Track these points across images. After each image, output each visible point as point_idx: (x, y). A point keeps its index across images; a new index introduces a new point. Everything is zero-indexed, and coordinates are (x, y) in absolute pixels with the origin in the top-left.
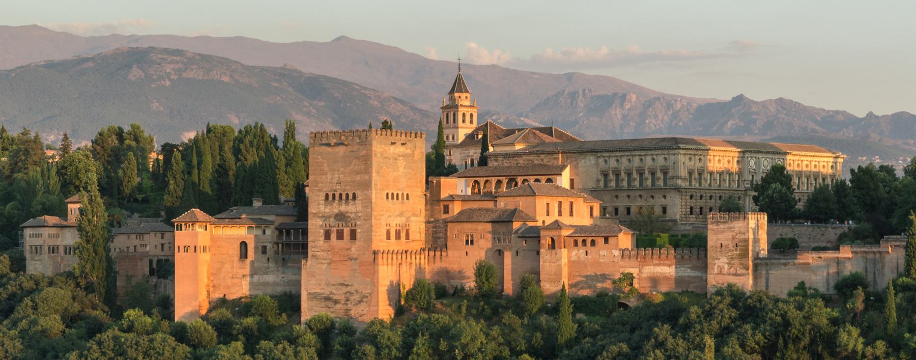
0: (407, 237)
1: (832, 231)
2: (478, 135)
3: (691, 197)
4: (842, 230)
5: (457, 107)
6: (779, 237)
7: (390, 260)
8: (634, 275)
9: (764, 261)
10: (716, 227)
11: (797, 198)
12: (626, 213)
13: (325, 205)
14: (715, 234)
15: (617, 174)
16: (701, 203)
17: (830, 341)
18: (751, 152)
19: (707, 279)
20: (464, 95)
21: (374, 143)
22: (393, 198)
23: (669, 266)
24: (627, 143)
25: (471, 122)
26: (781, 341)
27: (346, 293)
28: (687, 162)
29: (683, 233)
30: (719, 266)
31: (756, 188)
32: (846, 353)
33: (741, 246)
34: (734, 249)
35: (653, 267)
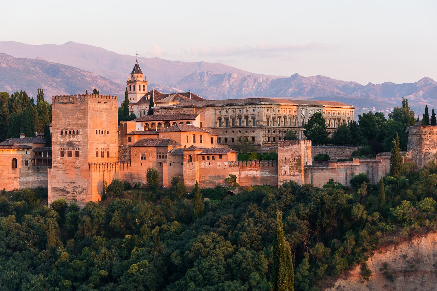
0: (108, 155)
1: (348, 151)
3: (269, 132)
4: (354, 150)
5: (135, 81)
6: (318, 154)
7: (98, 169)
8: (237, 176)
10: (282, 149)
11: (328, 132)
12: (232, 141)
13: (61, 137)
14: (282, 152)
15: (227, 119)
16: (274, 135)
17: (348, 212)
18: (302, 106)
21: (89, 102)
22: (99, 133)
23: (257, 171)
24: (232, 101)
25: (144, 90)
26: (320, 213)
27: (73, 187)
28: (266, 112)
29: (264, 152)
30: (284, 171)
31: (305, 126)
32: (357, 219)
33: (297, 159)
34: (293, 161)
35: (247, 171)
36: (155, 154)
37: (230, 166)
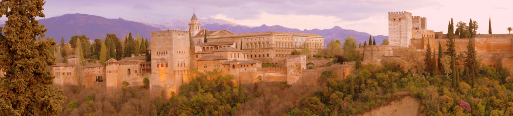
0: (184, 66)
2: (201, 33)
3: (277, 51)
5: (194, 24)
7: (179, 74)
9: (306, 71)
12: (255, 57)
13: (157, 56)
15: (251, 44)
16: (280, 53)
18: (295, 36)
19: (286, 77)
20: (196, 20)
21: (173, 35)
22: (179, 53)
23: (274, 73)
25: (199, 29)
27: (165, 85)
30: (290, 73)
36: (212, 65)
37: (258, 70)
